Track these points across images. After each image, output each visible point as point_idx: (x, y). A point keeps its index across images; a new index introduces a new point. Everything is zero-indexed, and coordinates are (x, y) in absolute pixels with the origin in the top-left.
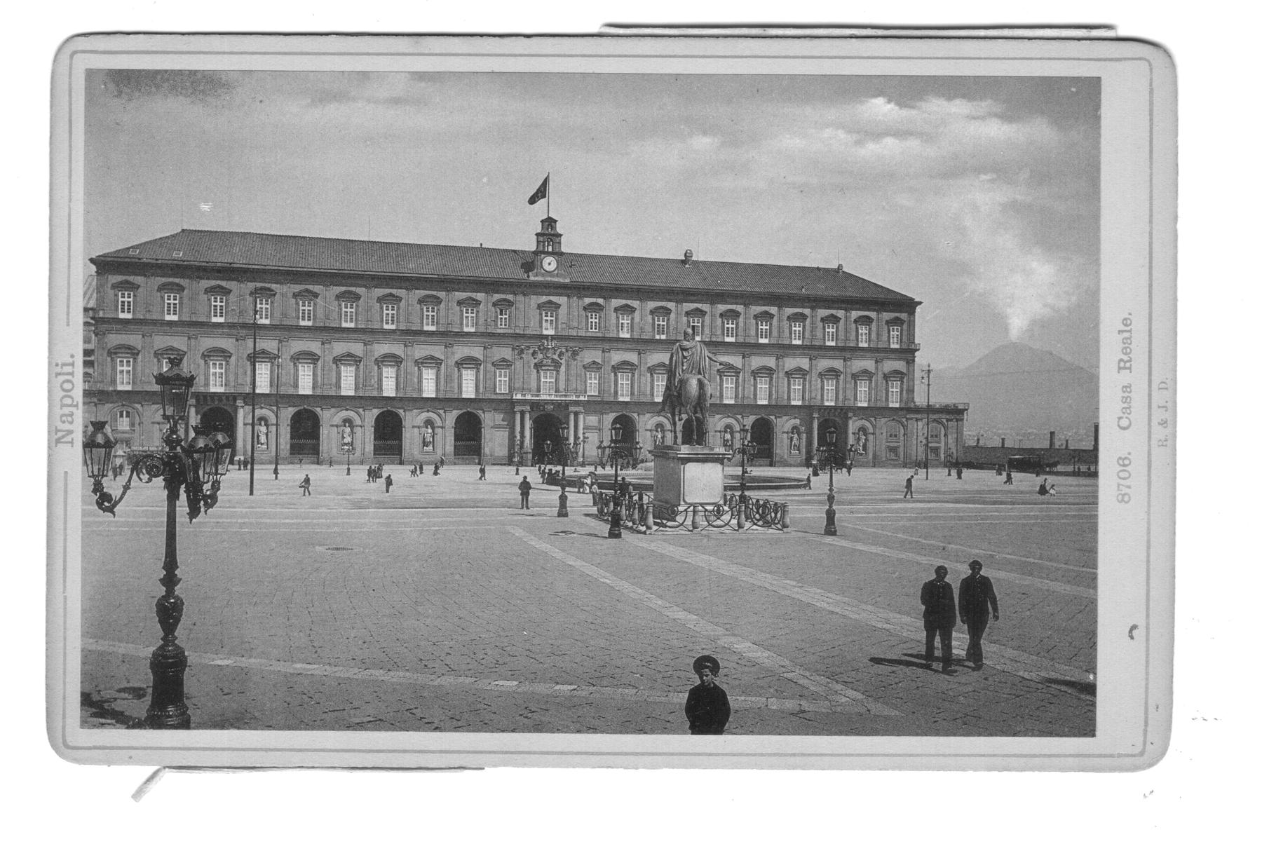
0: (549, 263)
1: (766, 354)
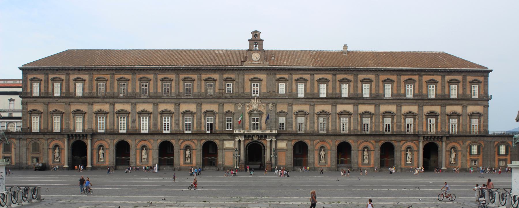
0: (256, 56)
1: (390, 104)
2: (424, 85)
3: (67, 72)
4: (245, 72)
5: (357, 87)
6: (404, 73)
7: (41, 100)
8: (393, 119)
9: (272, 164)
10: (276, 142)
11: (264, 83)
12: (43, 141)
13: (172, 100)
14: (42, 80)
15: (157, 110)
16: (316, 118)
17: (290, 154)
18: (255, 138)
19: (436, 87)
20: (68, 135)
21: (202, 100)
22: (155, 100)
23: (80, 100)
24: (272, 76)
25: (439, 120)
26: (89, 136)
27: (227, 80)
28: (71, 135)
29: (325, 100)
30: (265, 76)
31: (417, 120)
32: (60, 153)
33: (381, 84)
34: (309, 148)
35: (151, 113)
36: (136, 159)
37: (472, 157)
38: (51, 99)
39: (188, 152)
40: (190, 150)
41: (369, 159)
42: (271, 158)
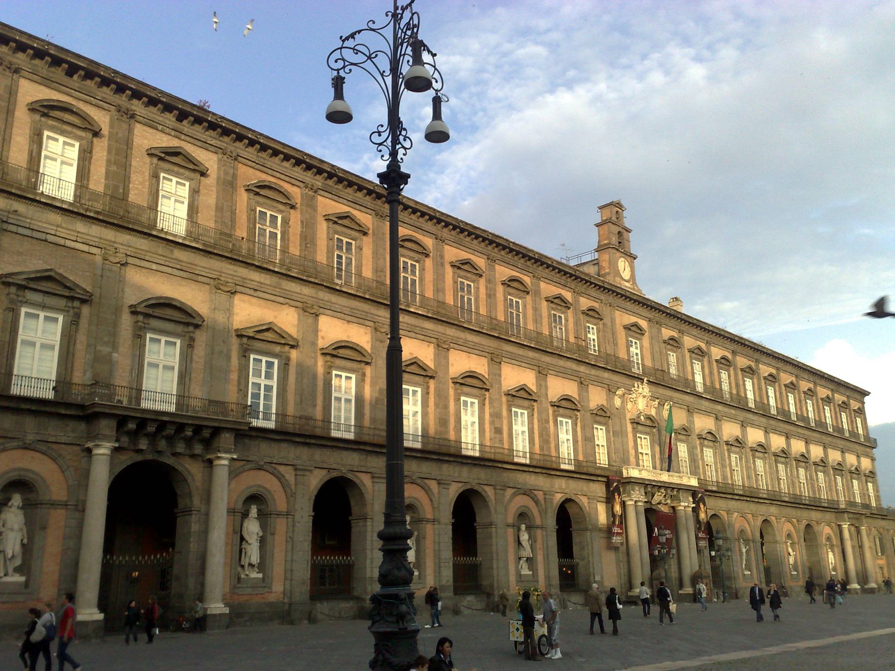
3: (122, 100)
4: (620, 301)
20: (122, 421)
26: (227, 438)
28: (136, 424)
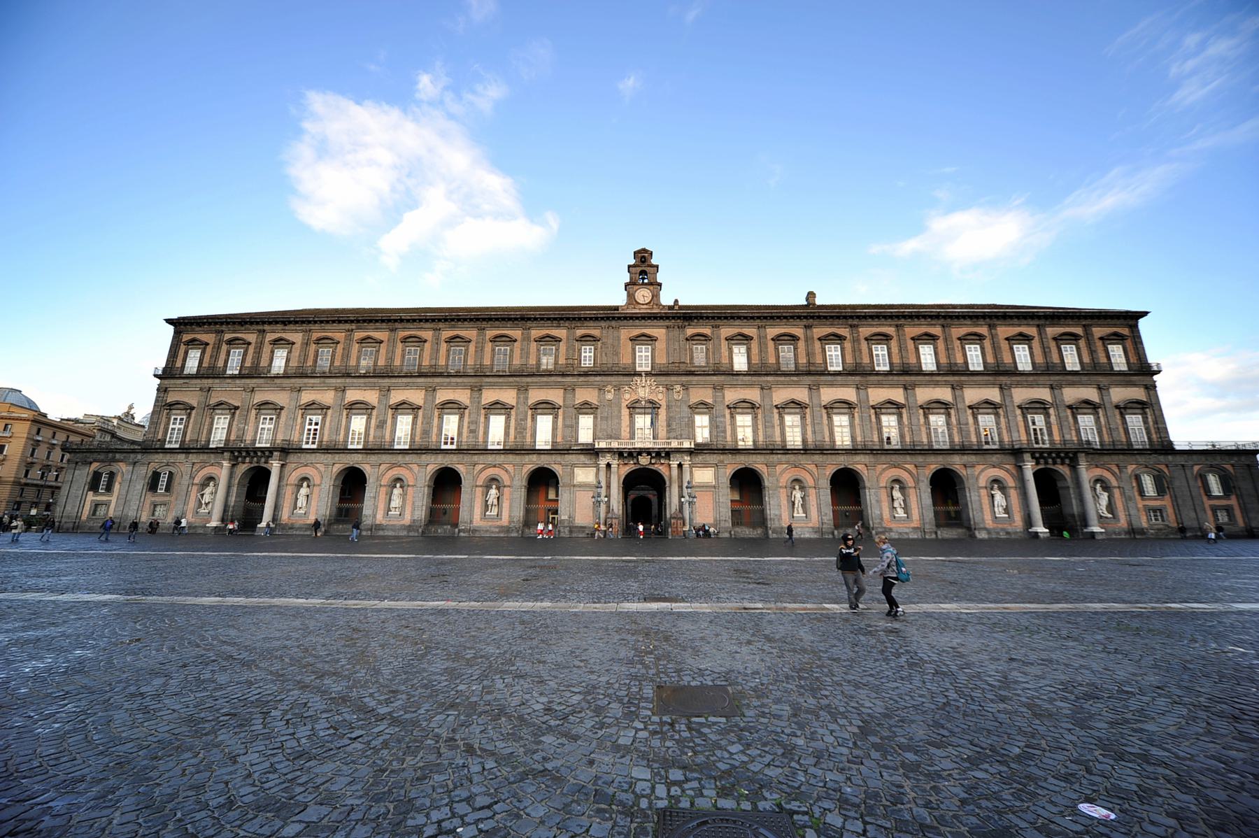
1: (937, 384)
2: (1004, 345)
3: (260, 327)
4: (622, 323)
5: (860, 351)
6: (956, 322)
7: (198, 381)
8: (948, 415)
9: (683, 519)
10: (691, 467)
11: (661, 345)
12: (183, 465)
13: (466, 380)
14: (207, 344)
15: (434, 401)
16: (776, 416)
17: (727, 496)
18: (644, 461)
19: (1030, 348)
21: (529, 380)
22: (429, 380)
23: (277, 381)
24: (676, 332)
25: (1053, 419)
27: (585, 339)
29: (795, 378)
30: (664, 331)
31: (1002, 419)
32: (214, 493)
33: (910, 344)
34: (766, 483)
35: (419, 408)
36: (376, 507)
37: (1147, 503)
38: (217, 381)
39: (493, 492)
40: (498, 488)
41: (906, 509)
42: (681, 504)
